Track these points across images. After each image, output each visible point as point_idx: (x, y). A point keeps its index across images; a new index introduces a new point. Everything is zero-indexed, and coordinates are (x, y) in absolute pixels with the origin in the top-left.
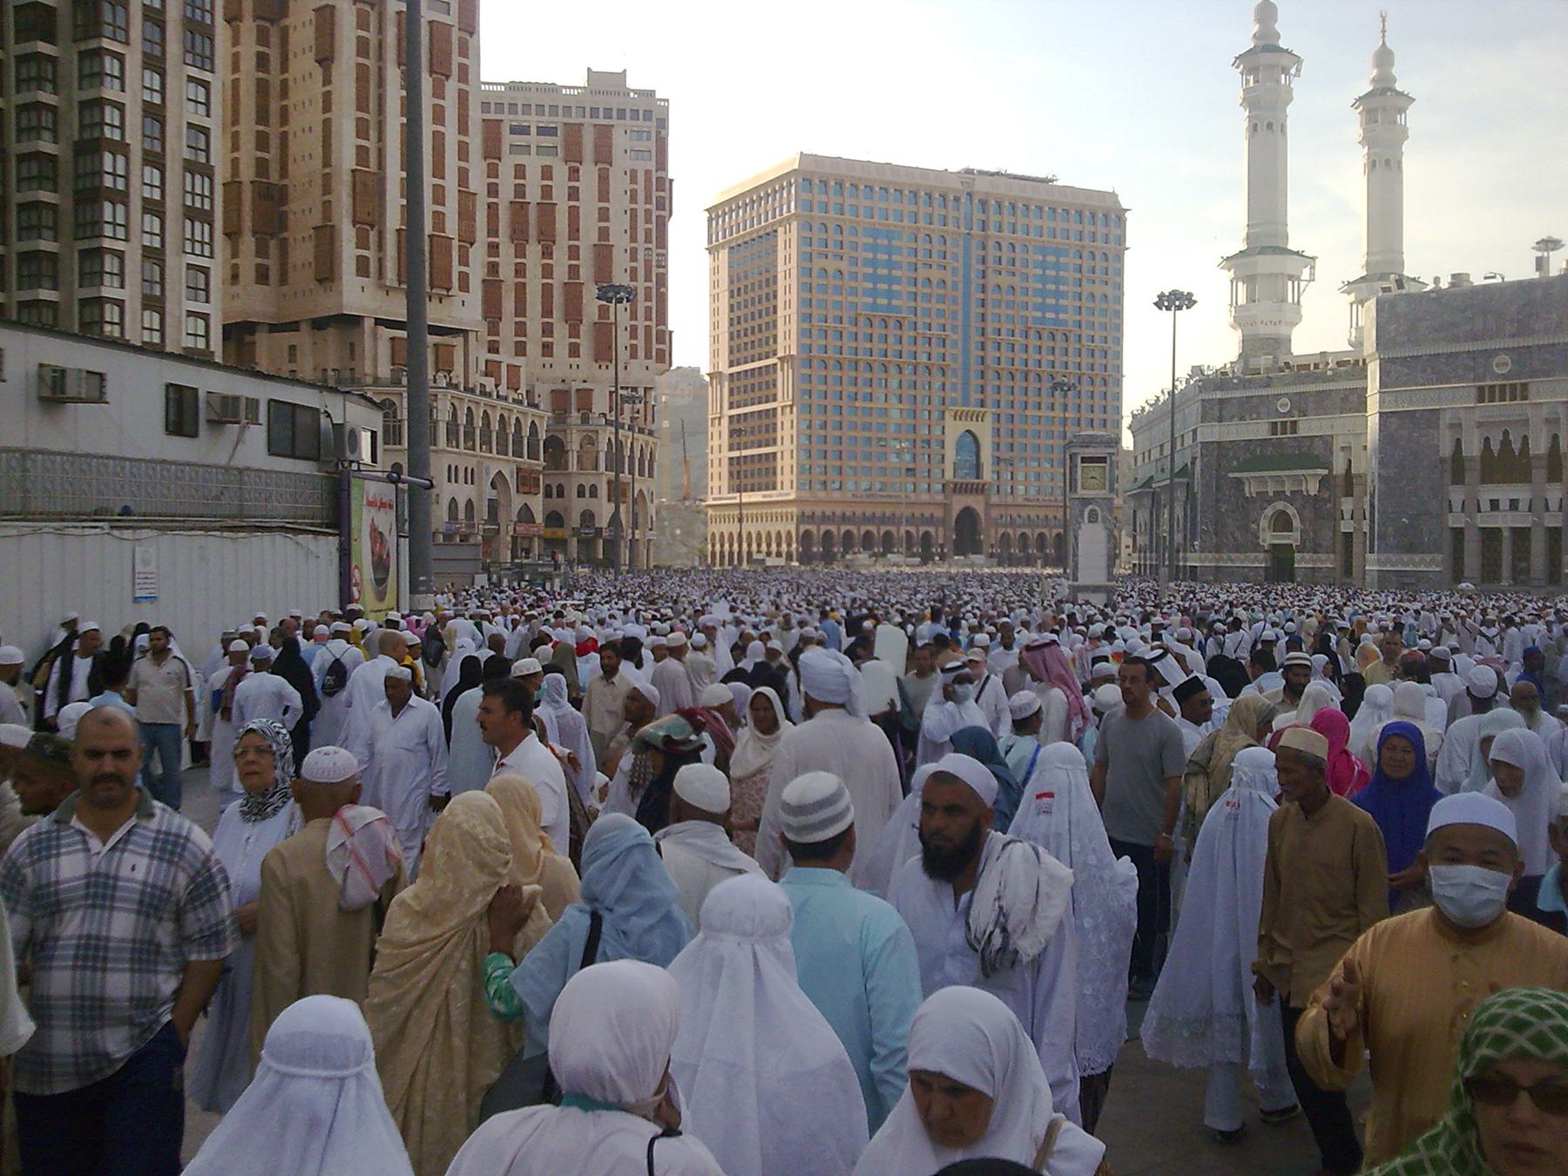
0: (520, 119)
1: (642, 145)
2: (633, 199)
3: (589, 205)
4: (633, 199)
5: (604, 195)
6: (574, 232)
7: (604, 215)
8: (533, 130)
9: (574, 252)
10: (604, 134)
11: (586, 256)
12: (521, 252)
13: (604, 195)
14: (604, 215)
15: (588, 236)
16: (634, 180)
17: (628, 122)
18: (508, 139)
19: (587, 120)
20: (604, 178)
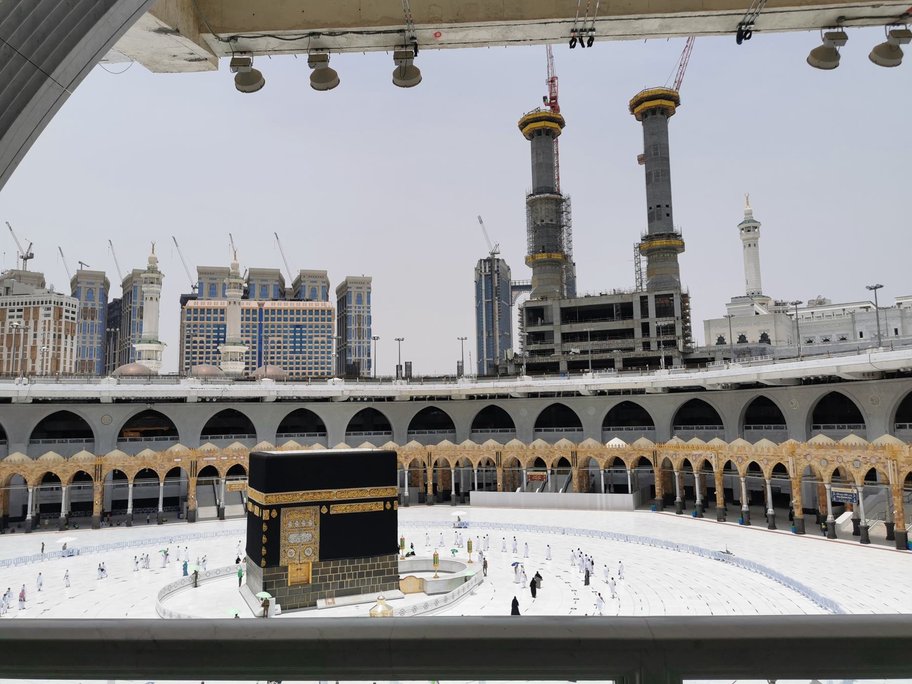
0: (12, 307)
1: (47, 312)
2: (44, 330)
3: (31, 333)
4: (44, 330)
5: (35, 330)
6: (25, 342)
7: (35, 336)
8: (16, 310)
9: (25, 349)
10: (36, 310)
11: (29, 349)
12: (9, 349)
13: (35, 330)
14: (35, 336)
15: (30, 342)
16: (45, 324)
17: (44, 305)
18: (9, 314)
19: (32, 305)
20: (36, 323)
